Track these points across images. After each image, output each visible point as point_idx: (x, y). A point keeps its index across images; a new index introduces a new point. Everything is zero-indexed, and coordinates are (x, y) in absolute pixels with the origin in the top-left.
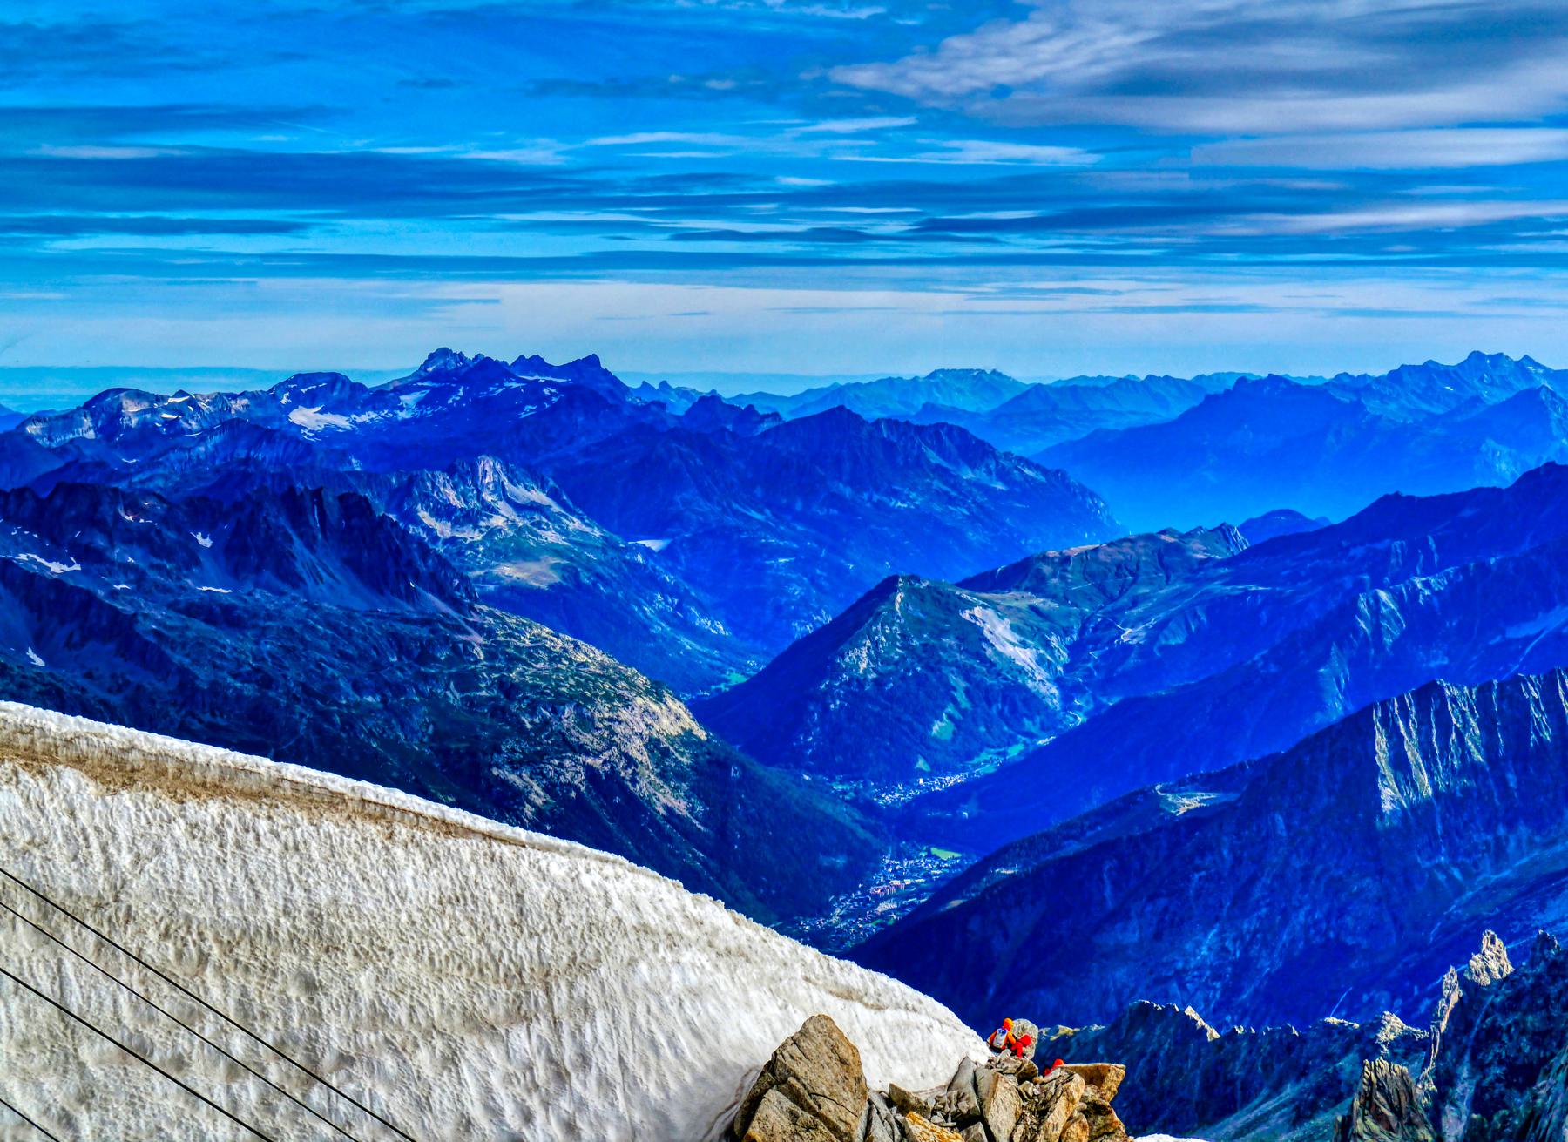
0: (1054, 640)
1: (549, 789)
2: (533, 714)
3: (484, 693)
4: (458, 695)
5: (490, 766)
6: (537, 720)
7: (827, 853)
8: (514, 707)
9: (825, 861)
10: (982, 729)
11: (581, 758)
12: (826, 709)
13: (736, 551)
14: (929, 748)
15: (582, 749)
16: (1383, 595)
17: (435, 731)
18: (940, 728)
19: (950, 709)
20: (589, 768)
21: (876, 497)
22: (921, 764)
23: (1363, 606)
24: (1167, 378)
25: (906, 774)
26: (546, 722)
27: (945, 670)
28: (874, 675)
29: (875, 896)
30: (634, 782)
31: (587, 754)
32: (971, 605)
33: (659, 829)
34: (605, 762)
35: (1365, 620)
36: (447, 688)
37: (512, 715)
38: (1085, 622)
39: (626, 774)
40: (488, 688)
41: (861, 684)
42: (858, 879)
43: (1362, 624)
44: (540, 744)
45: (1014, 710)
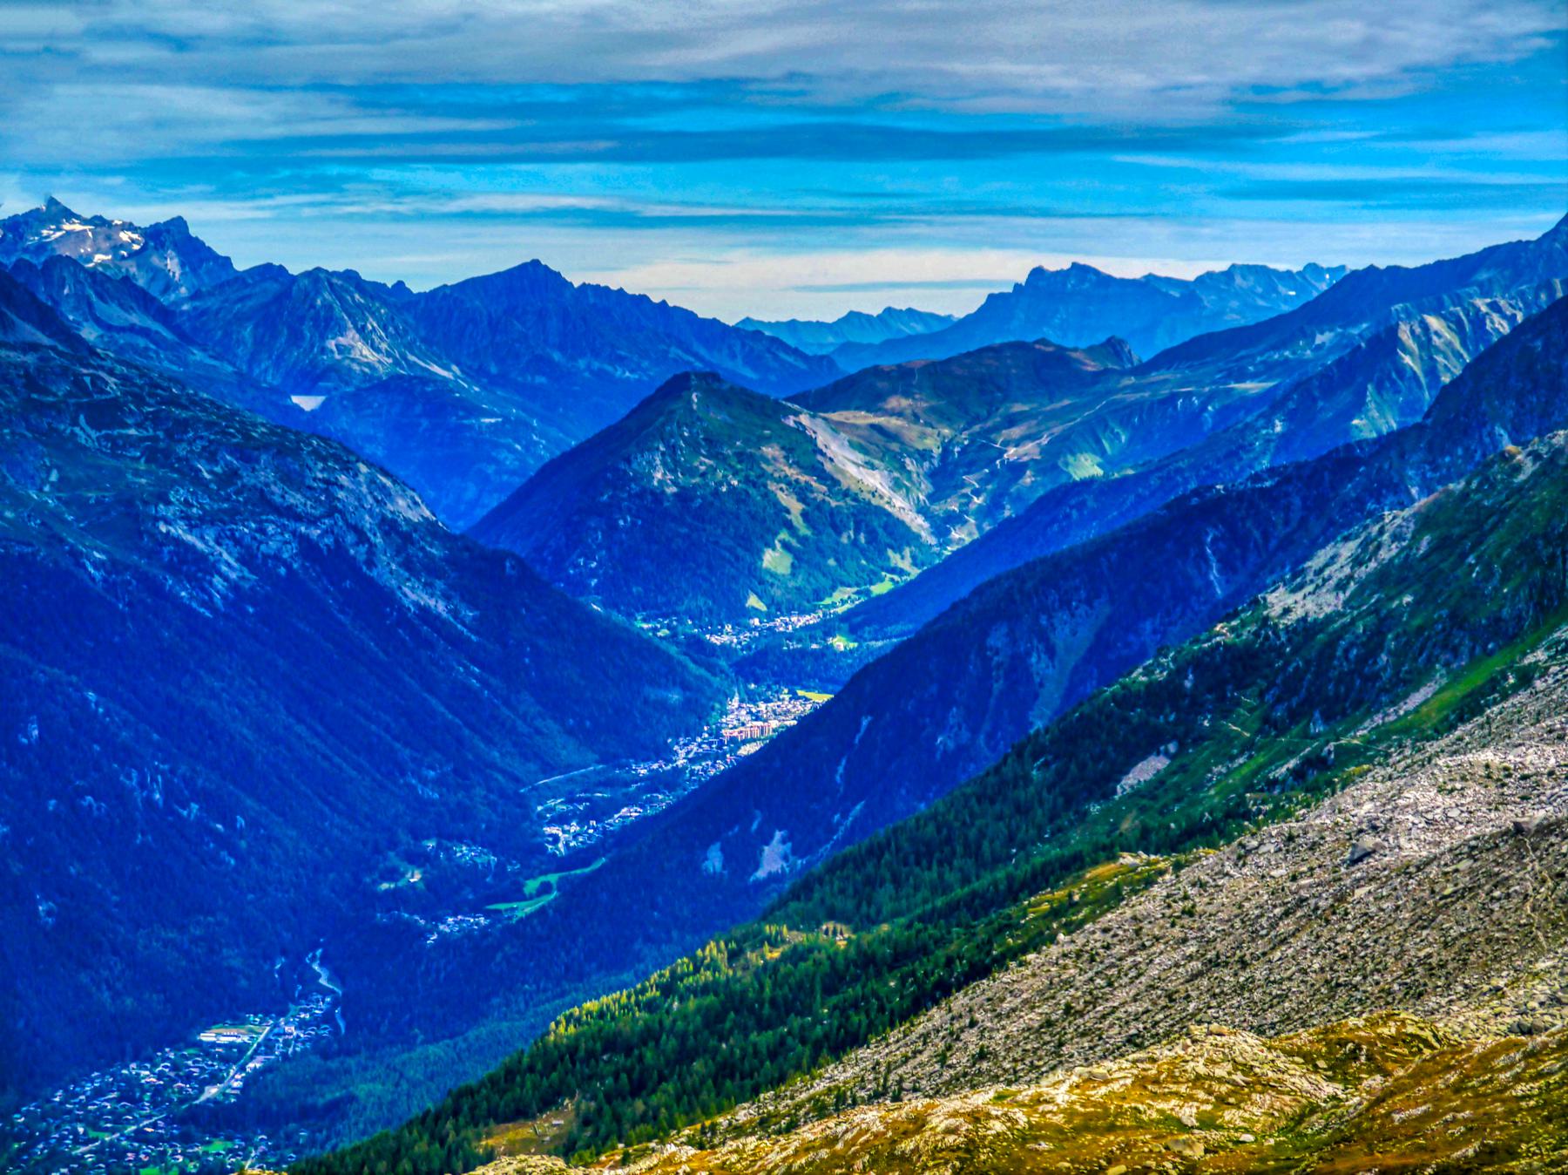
0: (911, 465)
1: (247, 559)
2: (212, 459)
3: (132, 432)
4: (94, 434)
5: (156, 519)
6: (218, 469)
7: (653, 683)
8: (182, 449)
9: (653, 693)
10: (832, 562)
11: (292, 525)
12: (613, 527)
13: (418, 409)
14: (761, 582)
15: (290, 513)
16: (1434, 322)
17: (61, 479)
18: (774, 560)
19: (784, 535)
20: (303, 539)
21: (596, 365)
22: (753, 601)
23: (1404, 334)
24: (910, 311)
25: (738, 615)
26: (233, 474)
27: (772, 486)
28: (674, 489)
29: (733, 740)
30: (370, 563)
31: (298, 518)
32: (796, 414)
33: (414, 632)
34: (325, 533)
35: (1411, 354)
36: (75, 423)
37: (179, 459)
38: (946, 451)
39: (358, 553)
40: (138, 426)
41: (658, 496)
42: (702, 717)
43: (1407, 360)
44: (228, 499)
45: (872, 537)
